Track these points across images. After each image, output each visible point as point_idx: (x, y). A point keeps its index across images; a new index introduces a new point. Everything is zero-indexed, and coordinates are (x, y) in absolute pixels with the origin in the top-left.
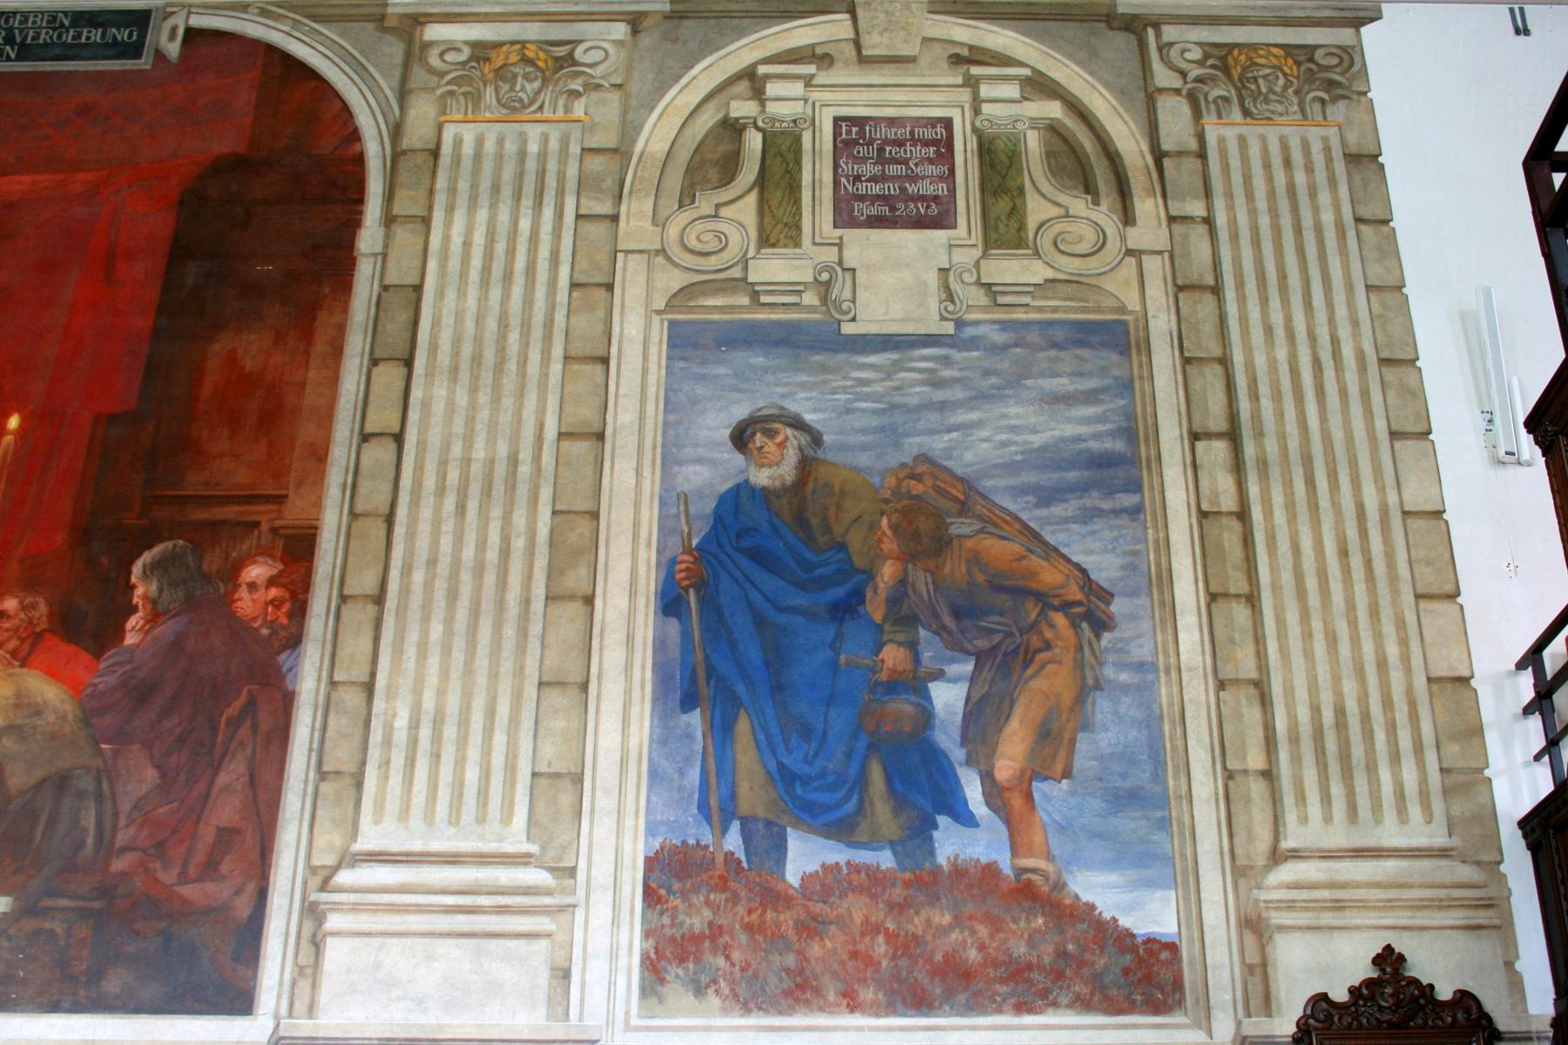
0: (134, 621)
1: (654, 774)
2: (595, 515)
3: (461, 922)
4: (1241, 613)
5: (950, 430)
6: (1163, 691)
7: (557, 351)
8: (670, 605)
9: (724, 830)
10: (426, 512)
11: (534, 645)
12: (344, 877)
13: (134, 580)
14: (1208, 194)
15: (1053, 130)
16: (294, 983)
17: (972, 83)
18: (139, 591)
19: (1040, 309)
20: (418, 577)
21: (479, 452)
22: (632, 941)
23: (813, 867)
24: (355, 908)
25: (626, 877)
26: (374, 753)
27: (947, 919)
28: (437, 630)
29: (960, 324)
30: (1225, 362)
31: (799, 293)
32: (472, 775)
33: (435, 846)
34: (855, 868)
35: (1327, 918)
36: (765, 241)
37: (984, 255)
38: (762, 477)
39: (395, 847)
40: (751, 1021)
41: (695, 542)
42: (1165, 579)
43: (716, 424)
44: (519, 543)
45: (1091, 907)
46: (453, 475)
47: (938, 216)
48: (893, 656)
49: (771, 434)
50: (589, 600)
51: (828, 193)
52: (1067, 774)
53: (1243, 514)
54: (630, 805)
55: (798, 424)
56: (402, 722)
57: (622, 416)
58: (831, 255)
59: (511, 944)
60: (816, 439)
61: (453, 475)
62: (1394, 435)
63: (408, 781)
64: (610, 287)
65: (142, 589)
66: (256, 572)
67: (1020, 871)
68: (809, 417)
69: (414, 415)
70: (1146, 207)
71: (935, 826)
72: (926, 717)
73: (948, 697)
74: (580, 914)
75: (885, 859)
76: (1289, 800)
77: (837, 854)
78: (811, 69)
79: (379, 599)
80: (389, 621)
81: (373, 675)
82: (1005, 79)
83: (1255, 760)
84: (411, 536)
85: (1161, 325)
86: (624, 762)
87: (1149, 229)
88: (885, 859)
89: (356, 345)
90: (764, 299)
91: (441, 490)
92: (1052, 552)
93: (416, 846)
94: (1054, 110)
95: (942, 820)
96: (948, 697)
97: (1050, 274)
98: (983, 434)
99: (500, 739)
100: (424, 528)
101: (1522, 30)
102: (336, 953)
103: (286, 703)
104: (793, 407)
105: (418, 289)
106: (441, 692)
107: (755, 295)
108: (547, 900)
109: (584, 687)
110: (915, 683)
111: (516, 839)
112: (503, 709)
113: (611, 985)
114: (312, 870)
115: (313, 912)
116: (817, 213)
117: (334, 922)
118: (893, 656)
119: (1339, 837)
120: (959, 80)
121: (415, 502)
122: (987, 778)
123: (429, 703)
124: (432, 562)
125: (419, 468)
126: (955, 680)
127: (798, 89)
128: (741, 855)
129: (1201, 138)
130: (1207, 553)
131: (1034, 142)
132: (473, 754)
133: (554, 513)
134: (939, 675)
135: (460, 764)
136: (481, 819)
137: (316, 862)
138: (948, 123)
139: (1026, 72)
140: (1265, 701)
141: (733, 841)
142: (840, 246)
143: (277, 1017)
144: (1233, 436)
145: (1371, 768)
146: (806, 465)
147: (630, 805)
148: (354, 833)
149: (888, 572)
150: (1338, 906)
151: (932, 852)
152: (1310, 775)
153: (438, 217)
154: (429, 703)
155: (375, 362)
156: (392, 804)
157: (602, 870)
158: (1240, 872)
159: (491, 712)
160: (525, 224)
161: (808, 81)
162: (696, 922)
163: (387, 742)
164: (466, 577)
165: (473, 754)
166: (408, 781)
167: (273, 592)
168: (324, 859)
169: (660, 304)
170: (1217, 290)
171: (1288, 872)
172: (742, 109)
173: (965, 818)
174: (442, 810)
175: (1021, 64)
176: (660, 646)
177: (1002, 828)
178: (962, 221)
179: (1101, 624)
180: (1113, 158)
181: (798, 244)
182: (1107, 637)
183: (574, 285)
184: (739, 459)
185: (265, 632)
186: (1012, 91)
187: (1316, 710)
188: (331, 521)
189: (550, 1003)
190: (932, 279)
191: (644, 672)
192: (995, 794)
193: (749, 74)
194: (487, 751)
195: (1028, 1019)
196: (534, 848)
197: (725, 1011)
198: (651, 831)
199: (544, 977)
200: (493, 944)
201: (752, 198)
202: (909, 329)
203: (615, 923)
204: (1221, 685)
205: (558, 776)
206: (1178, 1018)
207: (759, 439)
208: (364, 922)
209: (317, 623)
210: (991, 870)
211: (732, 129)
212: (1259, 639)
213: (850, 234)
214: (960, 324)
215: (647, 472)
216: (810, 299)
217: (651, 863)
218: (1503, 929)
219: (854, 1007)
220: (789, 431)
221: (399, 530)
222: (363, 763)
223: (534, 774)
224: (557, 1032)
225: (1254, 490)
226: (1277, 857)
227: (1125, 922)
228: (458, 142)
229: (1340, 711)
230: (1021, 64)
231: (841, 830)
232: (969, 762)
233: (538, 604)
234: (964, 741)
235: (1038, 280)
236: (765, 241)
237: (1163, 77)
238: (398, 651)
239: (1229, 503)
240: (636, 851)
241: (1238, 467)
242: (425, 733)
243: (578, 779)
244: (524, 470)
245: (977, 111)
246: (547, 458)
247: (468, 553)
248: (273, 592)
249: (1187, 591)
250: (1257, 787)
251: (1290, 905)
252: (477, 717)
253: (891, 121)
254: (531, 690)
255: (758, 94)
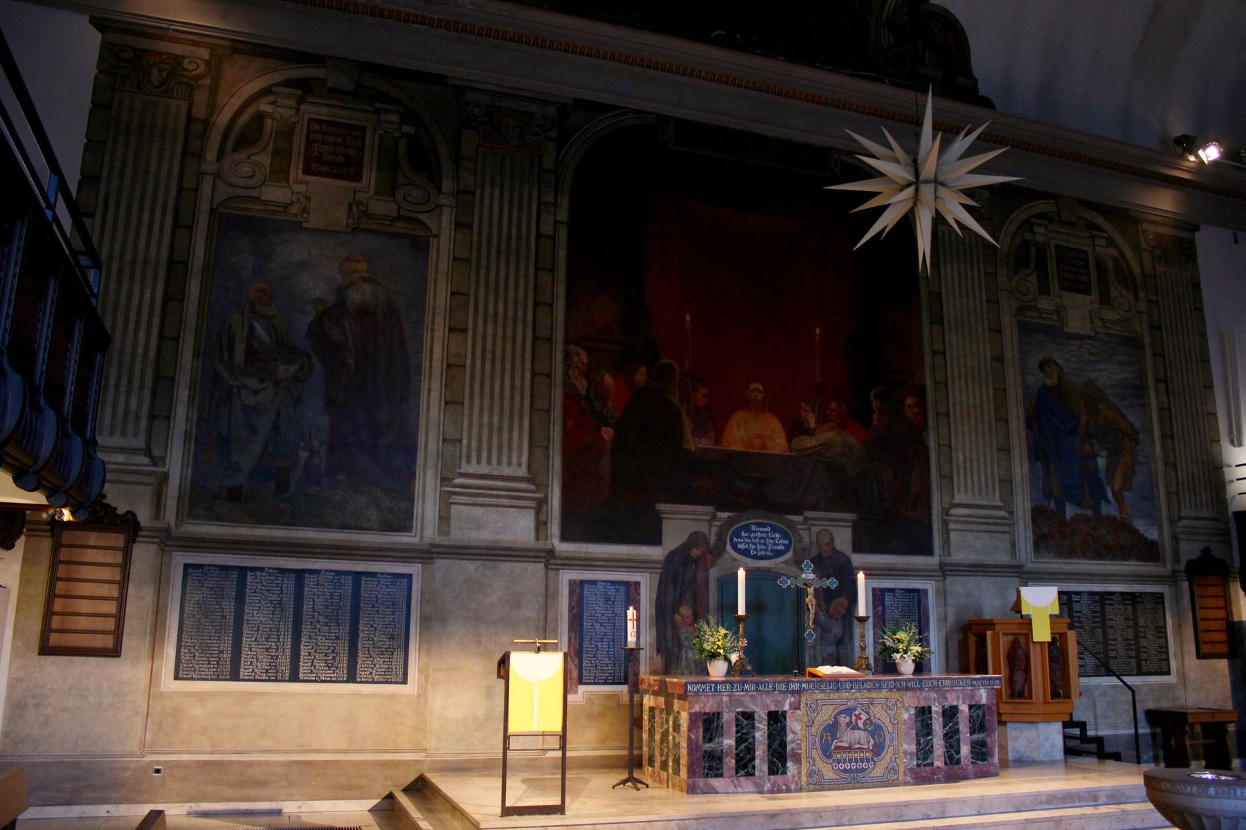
0: (875, 416)
1: (1031, 483)
2: (1005, 390)
3: (985, 527)
4: (1170, 441)
5: (1096, 371)
6: (1152, 464)
7: (986, 326)
8: (1029, 425)
9: (1050, 501)
10: (957, 384)
11: (994, 437)
12: (952, 511)
13: (872, 400)
14: (1157, 293)
15: (1115, 260)
16: (943, 545)
17: (1092, 237)
18: (874, 404)
19: (1116, 330)
20: (958, 408)
21: (969, 363)
22: (1030, 534)
23: (1072, 515)
24: (957, 522)
25: (1027, 515)
26: (955, 470)
27: (1105, 532)
28: (966, 428)
29: (1096, 333)
30: (1163, 355)
31: (1052, 314)
32: (983, 479)
33: (977, 502)
34: (1083, 515)
35: (1191, 537)
36: (1041, 293)
37: (1100, 308)
38: (1049, 382)
39: (965, 502)
40: (1061, 561)
41: (1033, 403)
42: (1151, 429)
43: (1034, 362)
44: (985, 399)
45: (1138, 530)
46: (963, 371)
47: (1087, 292)
48: (1087, 447)
49: (1050, 367)
50: (1007, 421)
51: (1056, 276)
52: (1131, 489)
53: (1169, 409)
54: (1026, 493)
55: (1057, 364)
56: (961, 460)
57: (1008, 355)
58: (1059, 300)
59: (999, 535)
60: (1061, 370)
61: (963, 371)
62: (1205, 386)
63: (966, 480)
64: (998, 303)
65: (876, 404)
66: (909, 401)
67: (1121, 518)
68: (1059, 362)
69: (947, 346)
70: (1141, 294)
71: (1100, 503)
72: (1097, 467)
73: (1101, 462)
74: (1016, 526)
75: (1089, 513)
76: (1182, 502)
77: (1078, 511)
78: (1045, 222)
79: (948, 415)
80: (952, 423)
81: (950, 443)
82: (1102, 237)
83: (1174, 489)
84: (954, 392)
85: (1147, 340)
86: (1022, 477)
87: (1142, 306)
88: (1089, 513)
89: (925, 315)
90: (1044, 315)
91: (960, 376)
92: (1123, 416)
93: (970, 502)
94: (1114, 252)
95: (1103, 502)
96: (1101, 462)
97: (1118, 317)
98: (1105, 374)
99: (989, 468)
100: (957, 390)
101: (1236, 242)
102: (953, 536)
103: (926, 450)
104: (1055, 358)
105: (940, 294)
106: (971, 450)
107: (1040, 313)
108: (1007, 521)
109: (1009, 451)
110: (1092, 457)
111: (998, 503)
112: (989, 457)
113: (1026, 549)
114: (943, 509)
115: (945, 523)
116: (1054, 285)
117: (952, 526)
118: (1087, 447)
119: (1193, 513)
120: (1088, 235)
121: (953, 381)
122: (1113, 490)
123: (968, 454)
124: (961, 403)
125: (952, 367)
126: (1103, 457)
127: (1042, 230)
128: (1055, 509)
129: (1154, 269)
130: (1161, 420)
131: (1110, 264)
132: (982, 472)
133: (994, 389)
134: (1098, 455)
135: (979, 475)
136: (987, 494)
137: (944, 506)
138: (1086, 252)
139: (1106, 235)
140: (1176, 470)
141: (1052, 505)
142: (1061, 297)
143: (940, 557)
144: (1165, 381)
145: (1201, 494)
146: (1060, 378)
147: (1026, 493)
148: (953, 497)
149: (1084, 418)
150: (1193, 534)
151: (1100, 512)
152: (1187, 494)
153: (942, 264)
154: (968, 454)
155: (932, 323)
156: (963, 489)
157: (1020, 513)
158: (1172, 522)
159: (985, 459)
160: (969, 273)
161: (1046, 227)
162: (1045, 530)
163: (958, 464)
164: (972, 409)
165: (982, 472)
166: (966, 480)
167: (916, 409)
168: (946, 505)
169: (1013, 312)
170: (1160, 329)
171: (1183, 523)
172: (1028, 236)
173: (1108, 502)
174: (976, 491)
175: (1105, 232)
176: (1028, 438)
177: (1117, 505)
178: (1093, 292)
179: (1137, 442)
180: (1131, 273)
181: (1049, 294)
182: (1138, 447)
183: (988, 301)
184: (1041, 375)
185: (916, 424)
186: (1103, 242)
187: (1188, 473)
188: (929, 384)
189: (1012, 554)
190: (1087, 313)
191: (1025, 449)
192: (1115, 494)
193: (1027, 221)
194: (986, 472)
195: (1126, 563)
196: (1002, 505)
197: (1055, 558)
198: (1032, 500)
199: (1009, 546)
200: (994, 535)
201: (1035, 273)
202: (1082, 332)
203: (1025, 529)
204: (1166, 465)
205: (1004, 481)
206: (1159, 564)
207: (1046, 368)
208: (959, 526)
209: (931, 423)
210: (1114, 518)
211: (1025, 244)
212: (1174, 450)
213: (1065, 294)
214: (1096, 333)
215: (1017, 376)
216: (1055, 317)
217: (1033, 510)
218: (1229, 543)
219: (1086, 557)
220: (1054, 366)
221: (950, 391)
222: (952, 473)
223: (1000, 480)
224: (1014, 563)
225: (1172, 401)
226: (1180, 518)
227: (1146, 535)
228: (943, 233)
229: (1193, 475)
230: (1105, 232)
231: (1078, 504)
232: (1108, 484)
233: (993, 421)
234: (1106, 477)
235: (1114, 319)
236: (1041, 293)
237: (1144, 245)
238: (956, 435)
239: (1166, 406)
240: (1028, 506)
241: (1168, 394)
242: (968, 464)
243: (1011, 483)
244: (983, 372)
245: (1094, 250)
246: (989, 368)
247: (971, 401)
248: (916, 409)
249: (1157, 434)
250: (1175, 497)
251: (1182, 532)
252: (982, 460)
253: (1072, 249)
254: (995, 452)
255: (1032, 231)
